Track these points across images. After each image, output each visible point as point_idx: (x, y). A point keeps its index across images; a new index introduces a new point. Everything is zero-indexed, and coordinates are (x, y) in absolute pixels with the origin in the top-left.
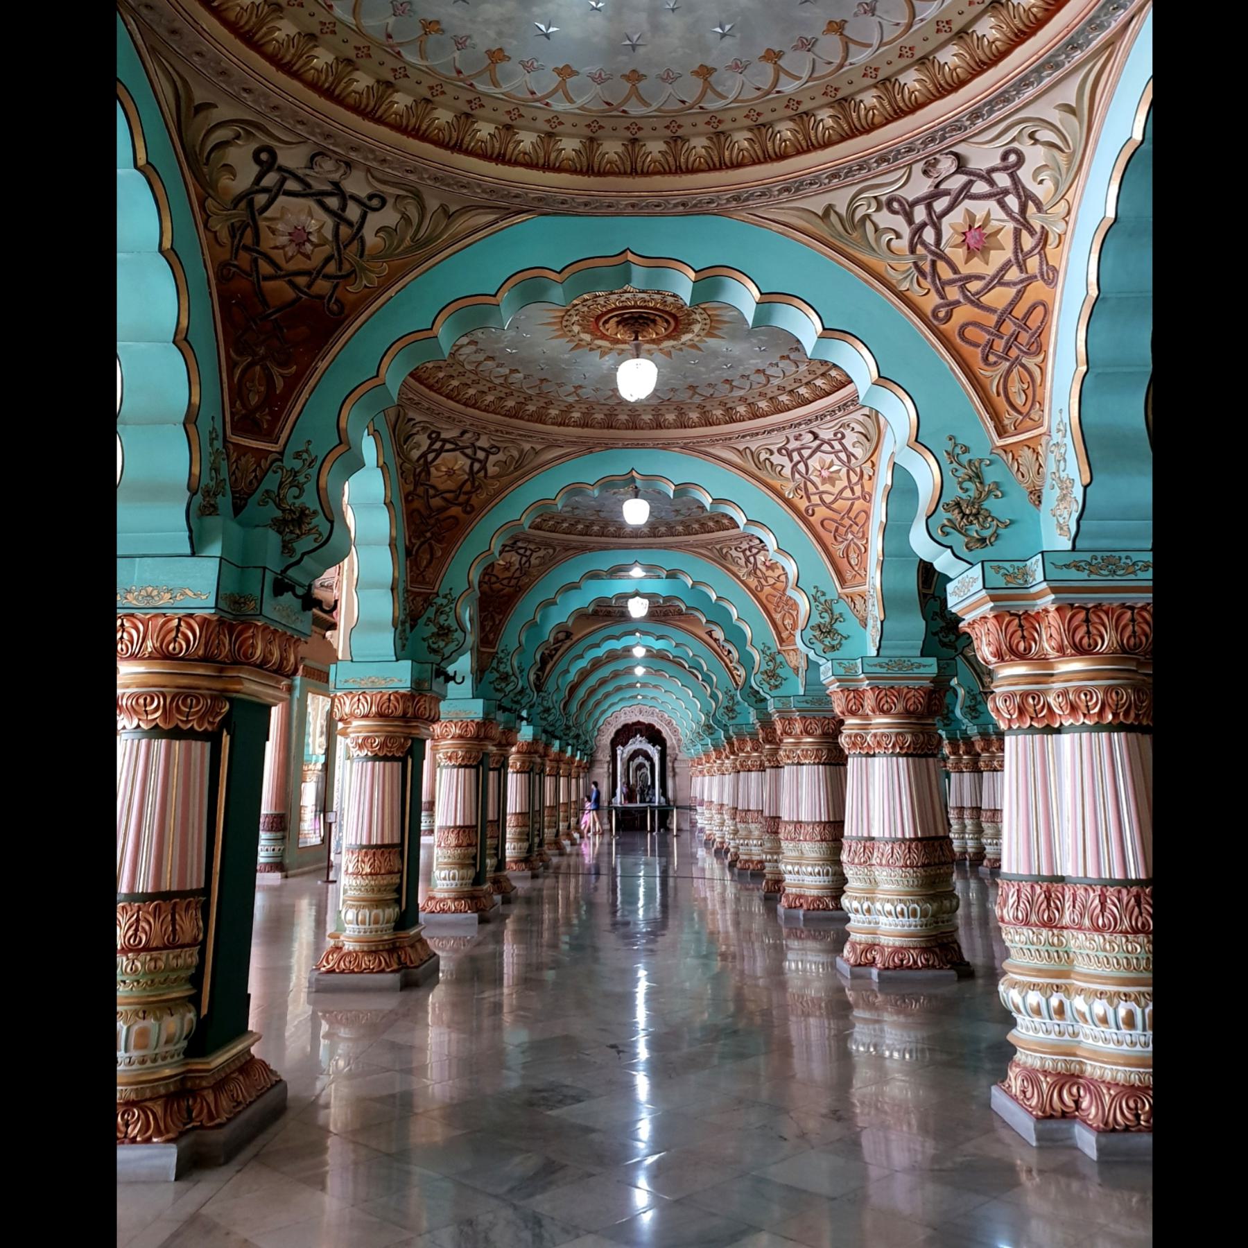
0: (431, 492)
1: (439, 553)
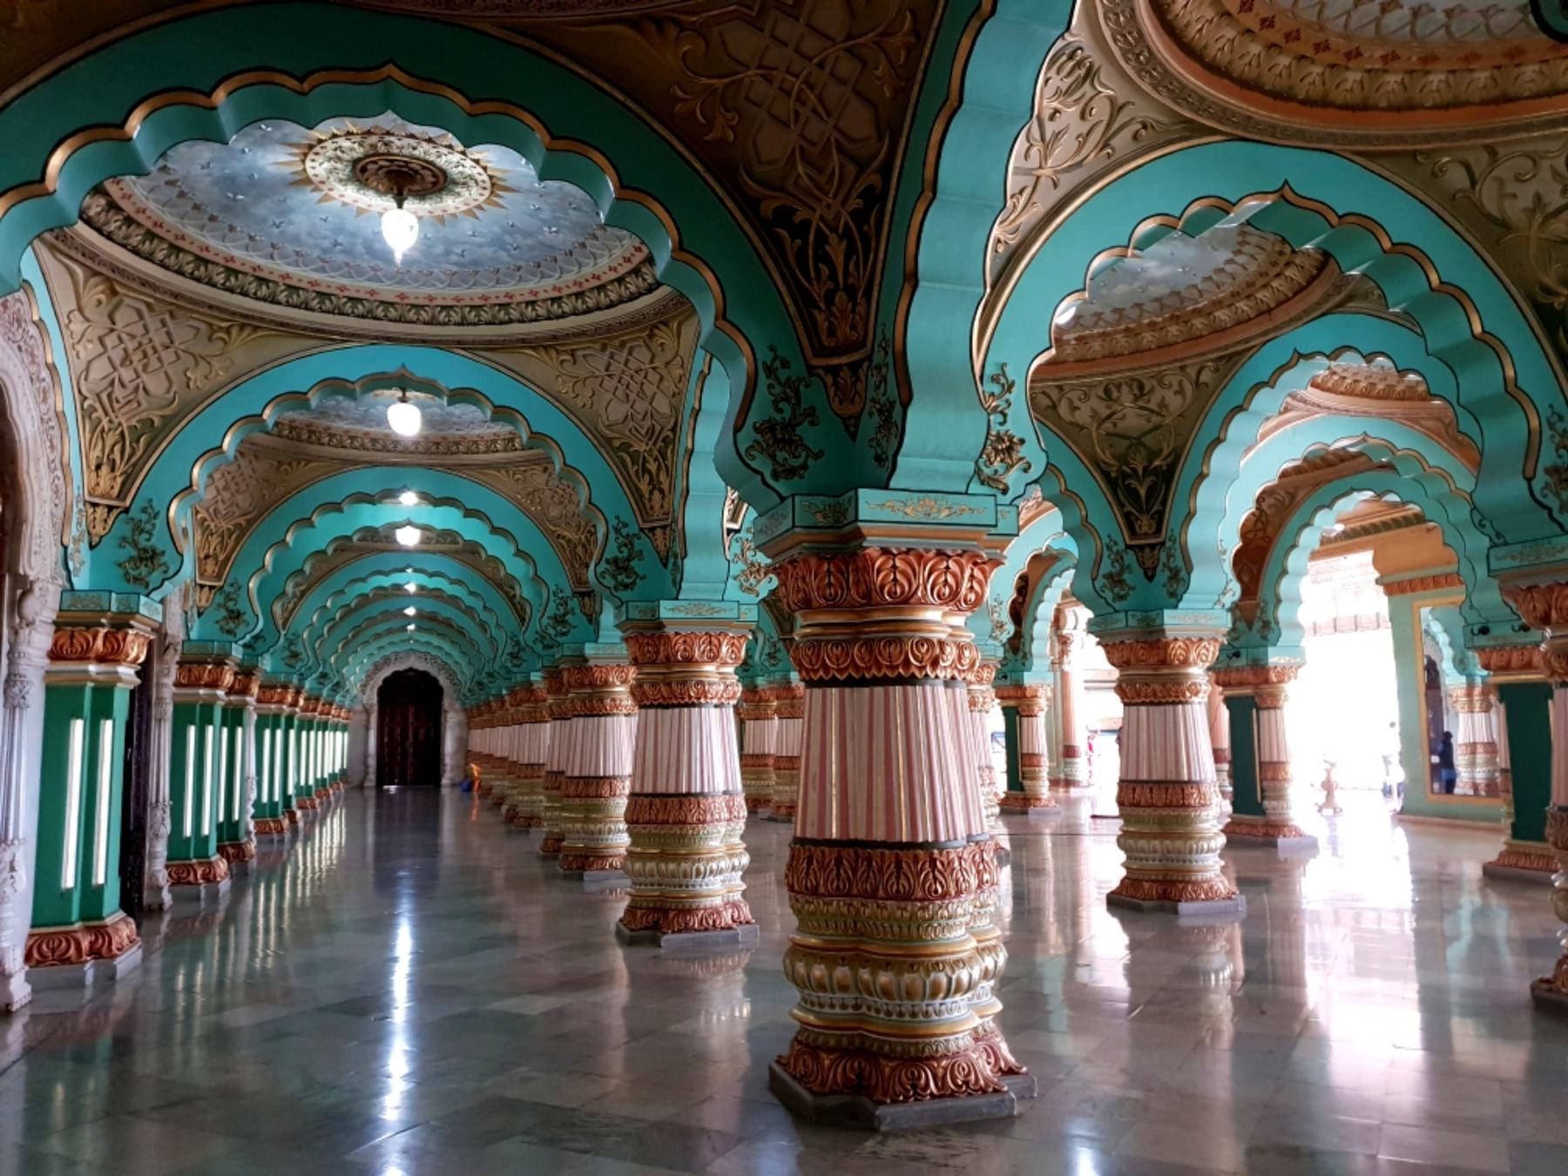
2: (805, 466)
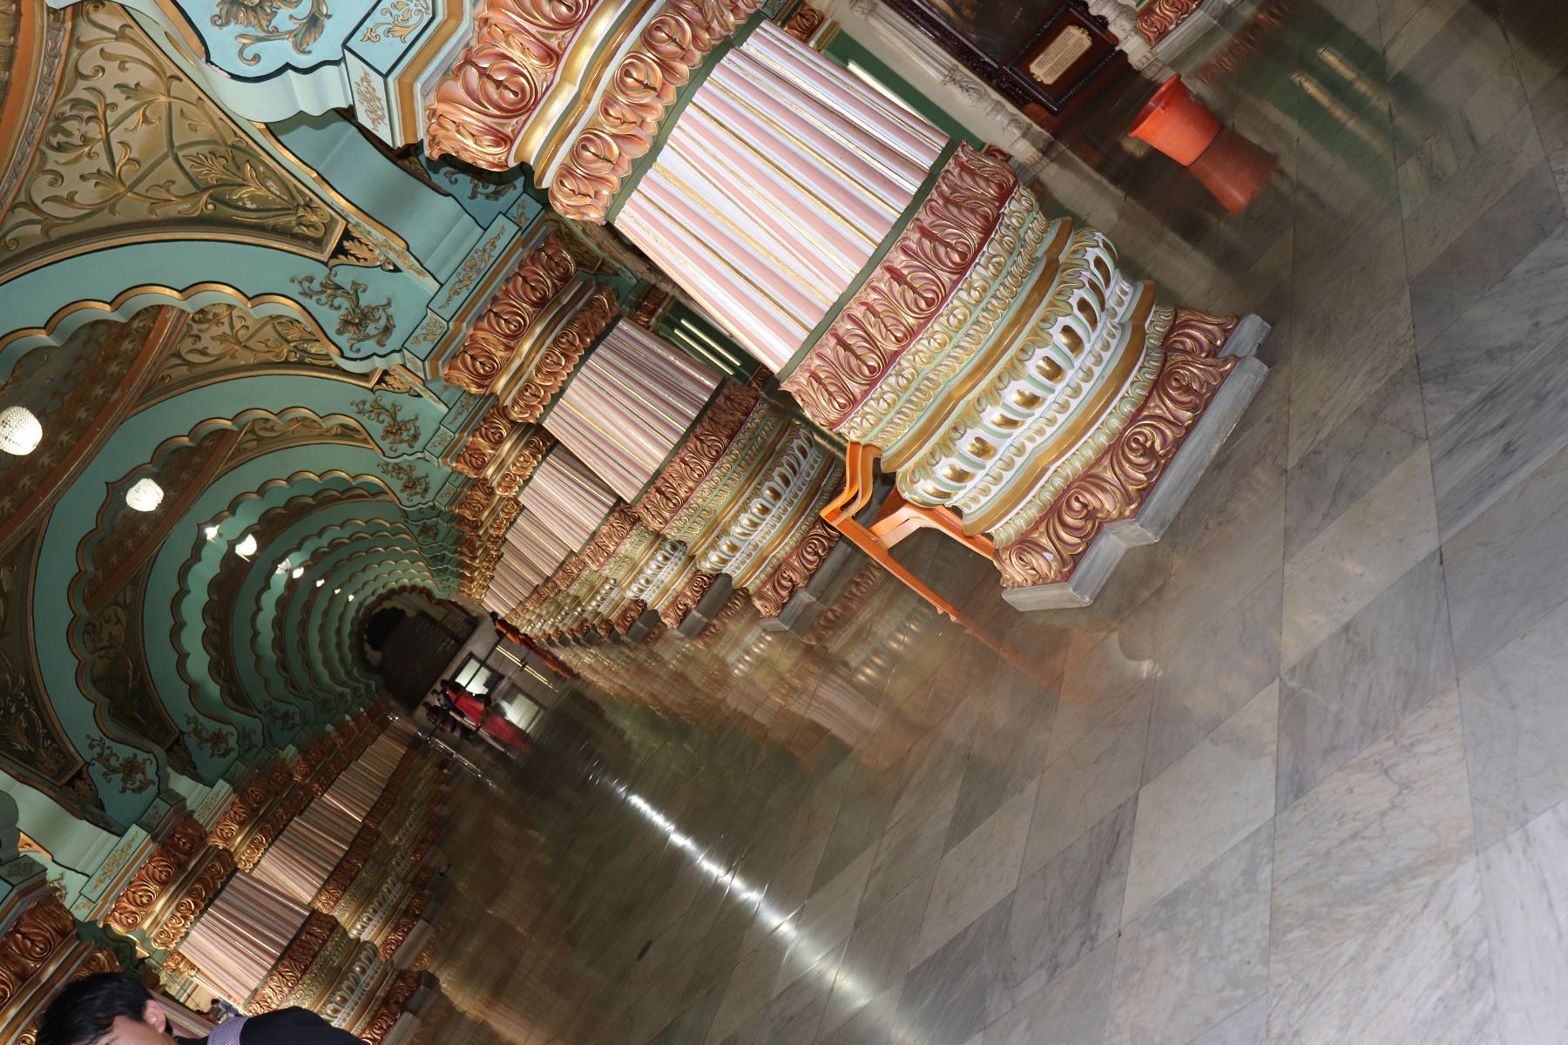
2: (389, 318)
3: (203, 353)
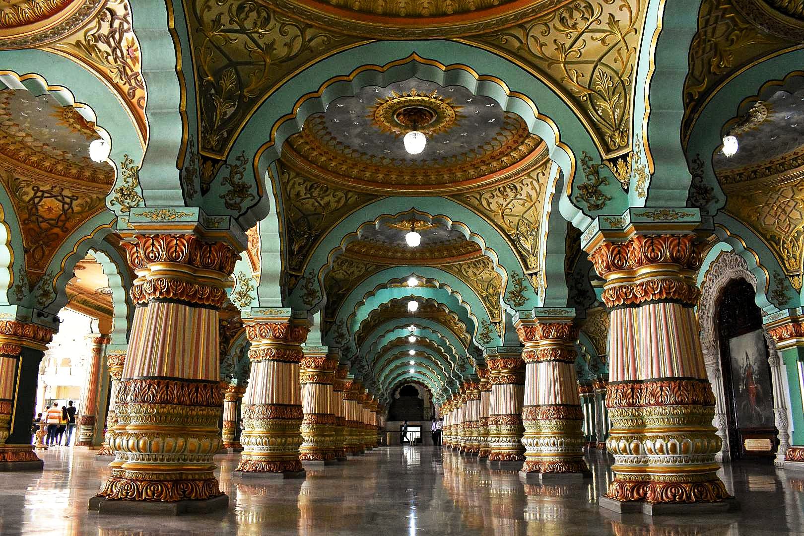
0: (40, 219)
1: (47, 252)
3: (489, 204)
